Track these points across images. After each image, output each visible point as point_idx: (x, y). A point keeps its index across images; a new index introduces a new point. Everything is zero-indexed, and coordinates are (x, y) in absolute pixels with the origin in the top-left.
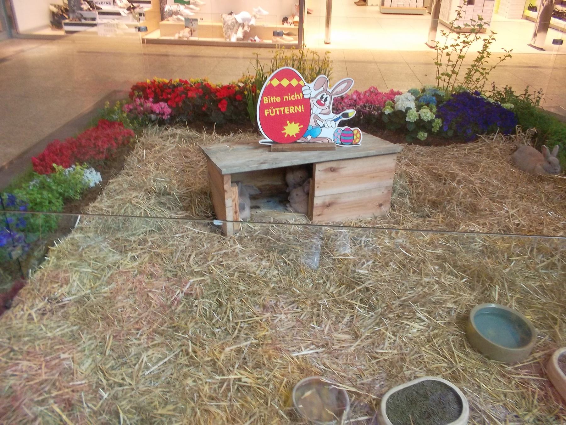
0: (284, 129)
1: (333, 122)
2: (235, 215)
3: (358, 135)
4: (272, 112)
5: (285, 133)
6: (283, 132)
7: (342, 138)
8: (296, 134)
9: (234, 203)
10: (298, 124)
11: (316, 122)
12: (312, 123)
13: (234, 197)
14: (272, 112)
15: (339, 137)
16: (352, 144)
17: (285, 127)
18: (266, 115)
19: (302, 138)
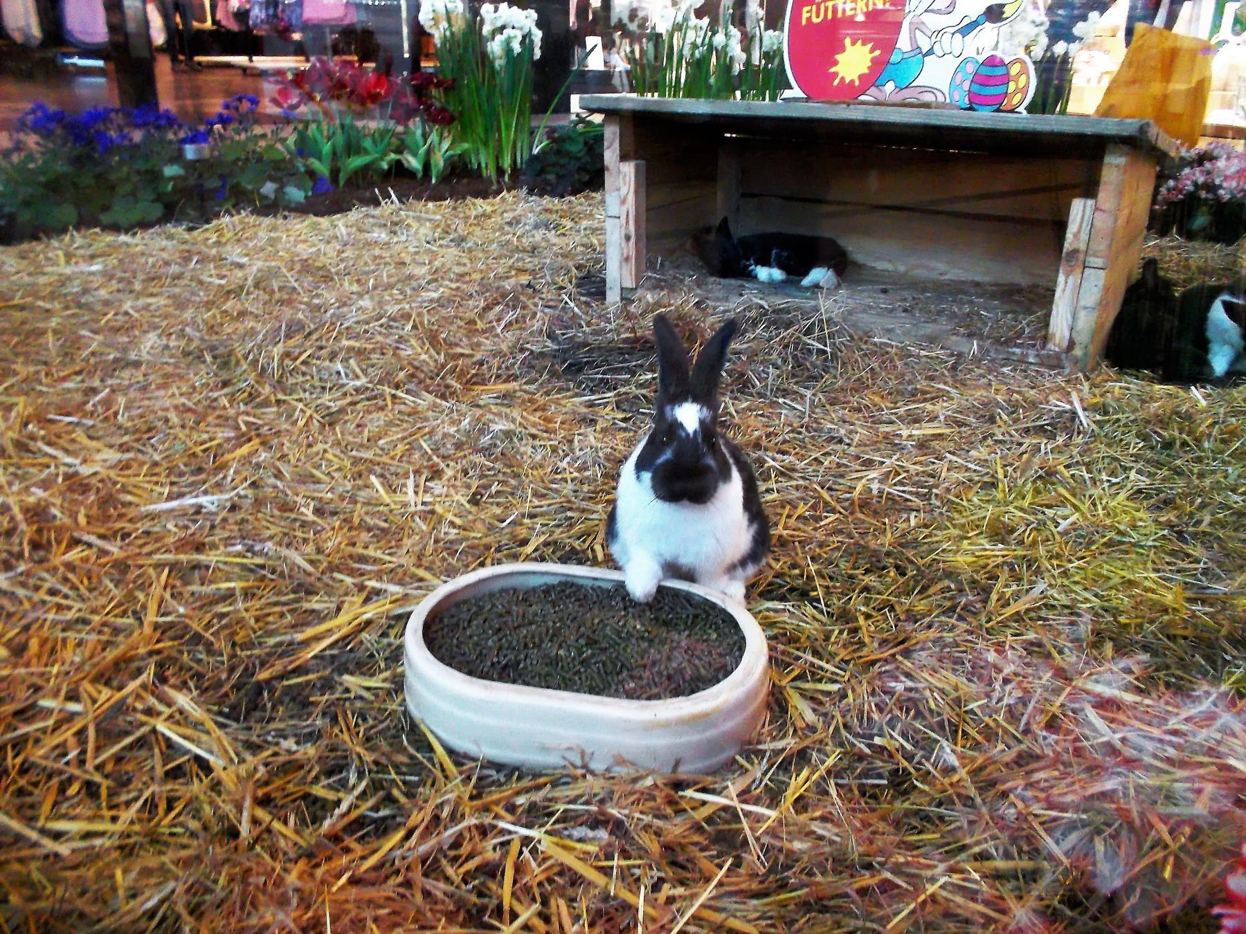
0: (835, 63)
1: (958, 36)
2: (624, 244)
3: (1022, 81)
4: (818, 16)
5: (835, 75)
6: (832, 70)
7: (976, 88)
8: (861, 77)
9: (624, 209)
10: (870, 45)
11: (913, 39)
12: (903, 43)
13: (624, 191)
14: (818, 16)
15: (966, 86)
16: (998, 110)
17: (838, 57)
18: (804, 22)
19: (873, 90)
